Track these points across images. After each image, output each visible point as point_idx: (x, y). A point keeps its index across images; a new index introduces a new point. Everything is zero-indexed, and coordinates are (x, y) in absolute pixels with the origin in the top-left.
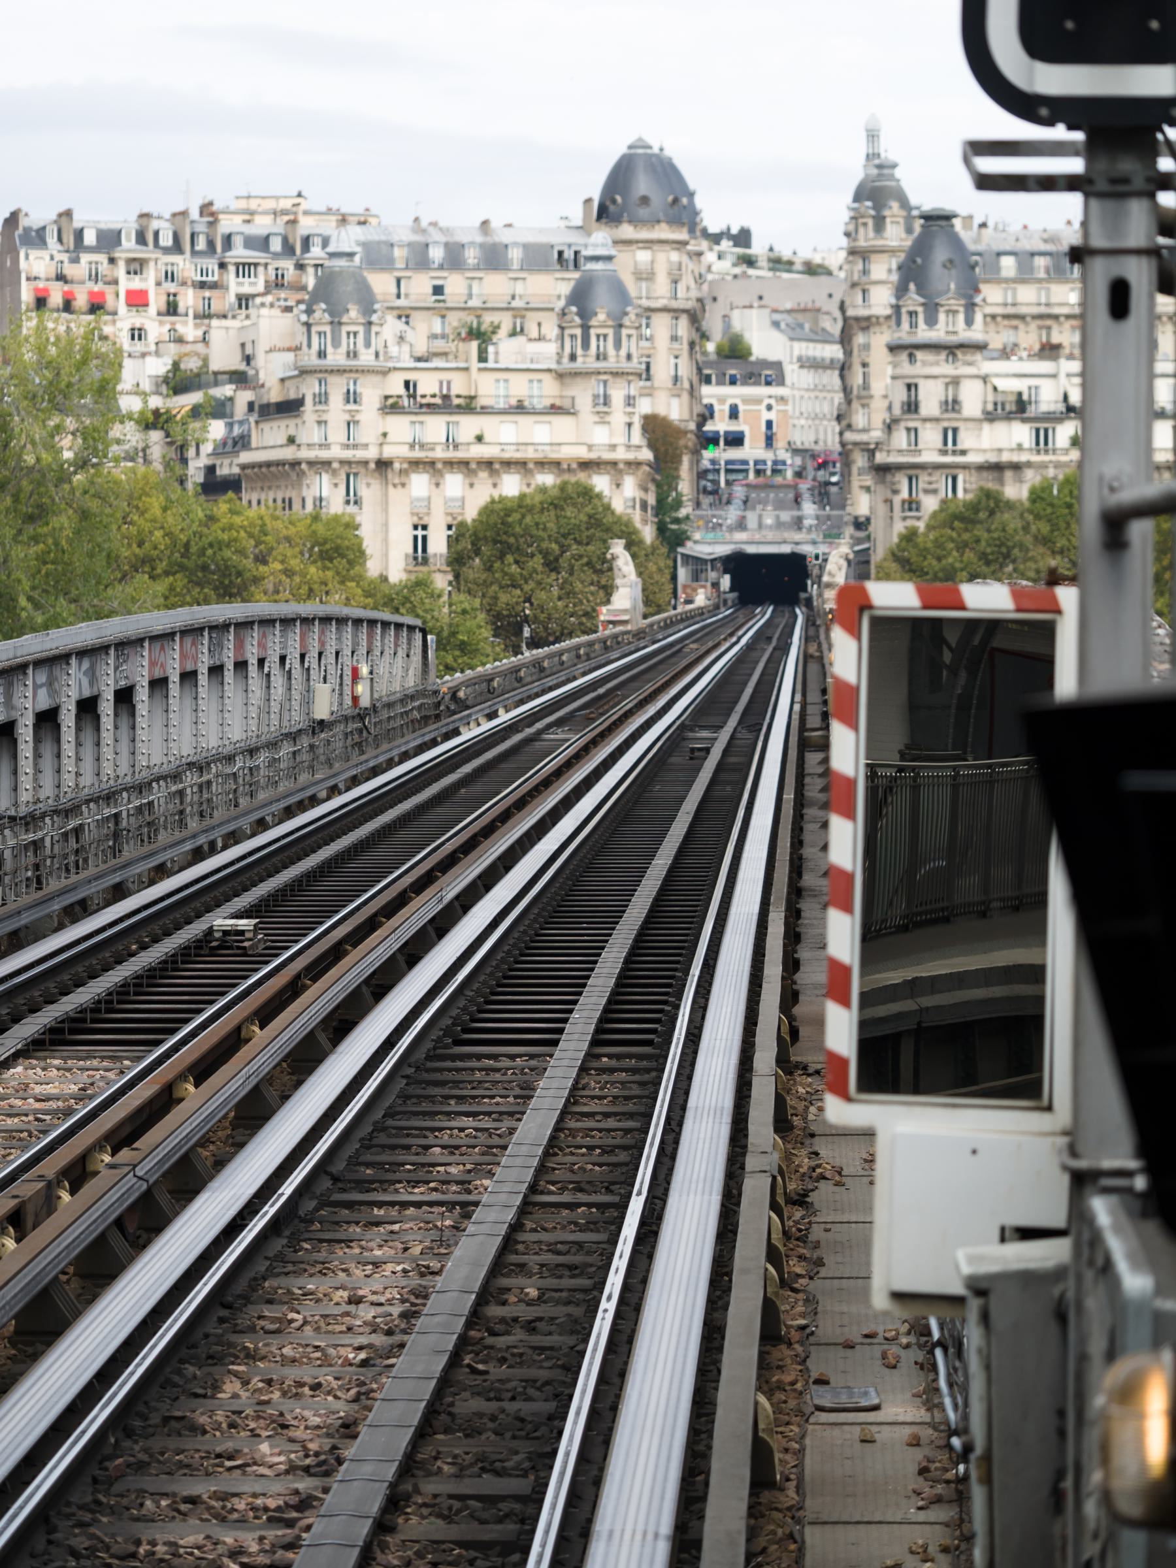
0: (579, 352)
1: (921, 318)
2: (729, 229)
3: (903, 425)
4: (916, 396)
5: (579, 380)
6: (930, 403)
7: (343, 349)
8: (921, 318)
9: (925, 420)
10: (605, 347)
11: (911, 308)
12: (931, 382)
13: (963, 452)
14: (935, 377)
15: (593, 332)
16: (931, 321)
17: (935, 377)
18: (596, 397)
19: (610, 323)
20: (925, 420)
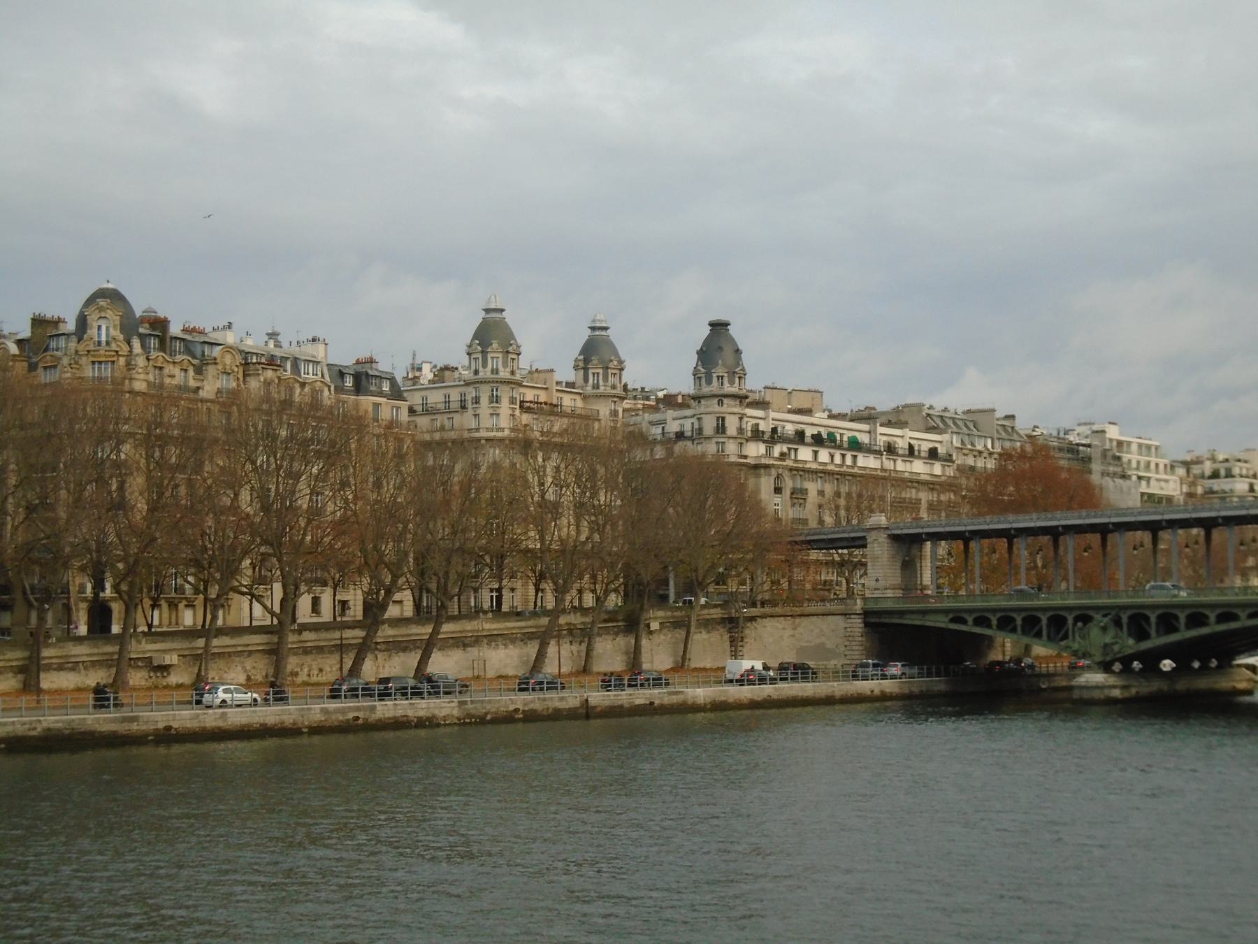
0: (601, 383)
3: (715, 440)
5: (601, 400)
6: (732, 429)
7: (509, 370)
9: (729, 438)
11: (720, 374)
12: (732, 416)
13: (746, 457)
14: (735, 414)
15: (609, 371)
16: (732, 383)
17: (735, 414)
18: (611, 410)
20: (729, 438)
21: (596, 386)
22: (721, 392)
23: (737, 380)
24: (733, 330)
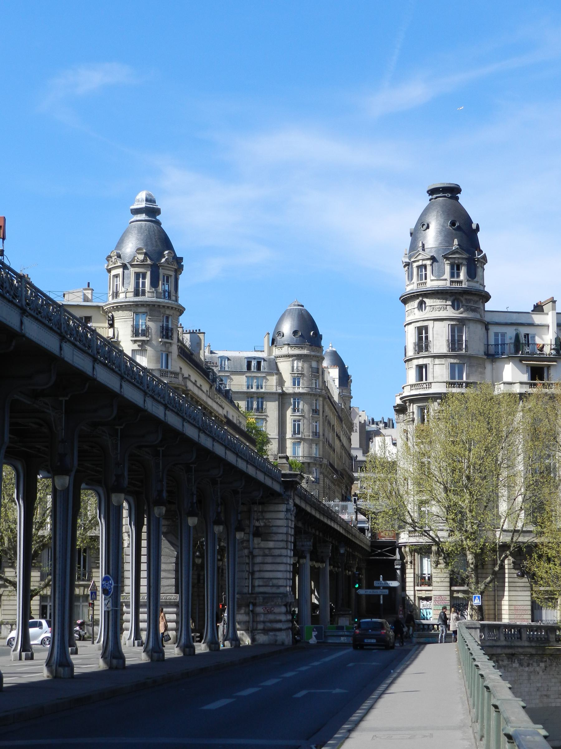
1: (429, 268)
2: (383, 418)
3: (416, 362)
4: (427, 338)
8: (429, 268)
9: (435, 357)
10: (144, 284)
11: (420, 263)
20: (435, 357)
22: (423, 288)
23: (447, 268)
24: (463, 199)
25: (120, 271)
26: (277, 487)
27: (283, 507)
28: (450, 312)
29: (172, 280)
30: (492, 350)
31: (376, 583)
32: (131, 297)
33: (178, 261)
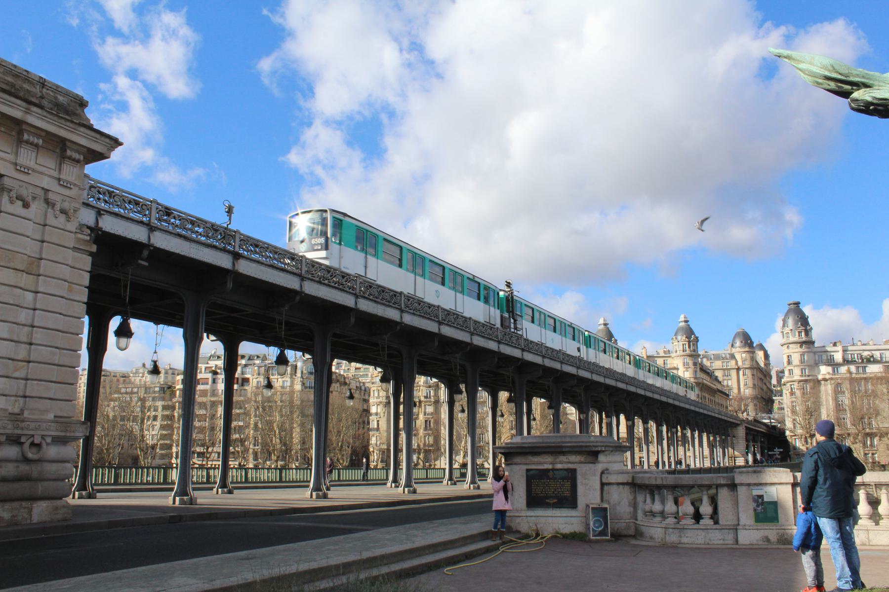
12: (796, 354)
19: (687, 340)
21: (676, 352)
22: (789, 341)
23: (797, 334)
24: (801, 306)
25: (677, 343)
26: (739, 422)
27: (741, 428)
28: (800, 350)
29: (695, 345)
30: (817, 362)
31: (775, 450)
32: (682, 353)
33: (697, 338)
